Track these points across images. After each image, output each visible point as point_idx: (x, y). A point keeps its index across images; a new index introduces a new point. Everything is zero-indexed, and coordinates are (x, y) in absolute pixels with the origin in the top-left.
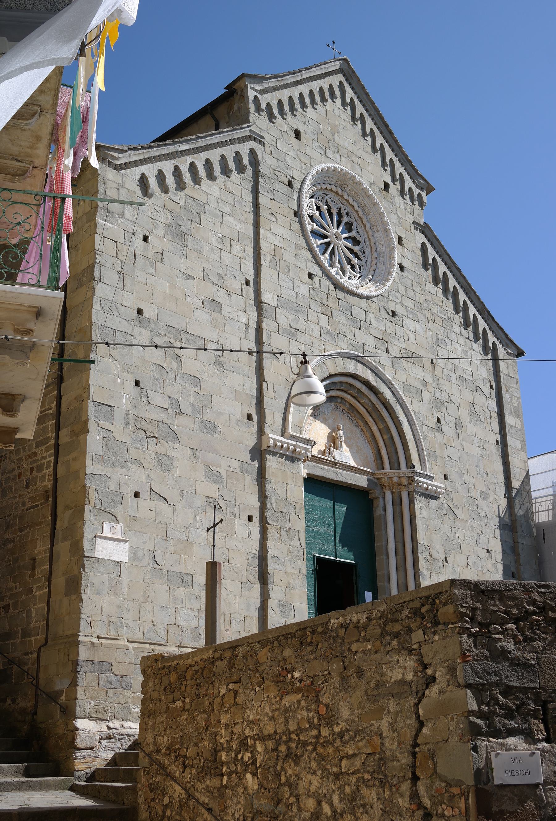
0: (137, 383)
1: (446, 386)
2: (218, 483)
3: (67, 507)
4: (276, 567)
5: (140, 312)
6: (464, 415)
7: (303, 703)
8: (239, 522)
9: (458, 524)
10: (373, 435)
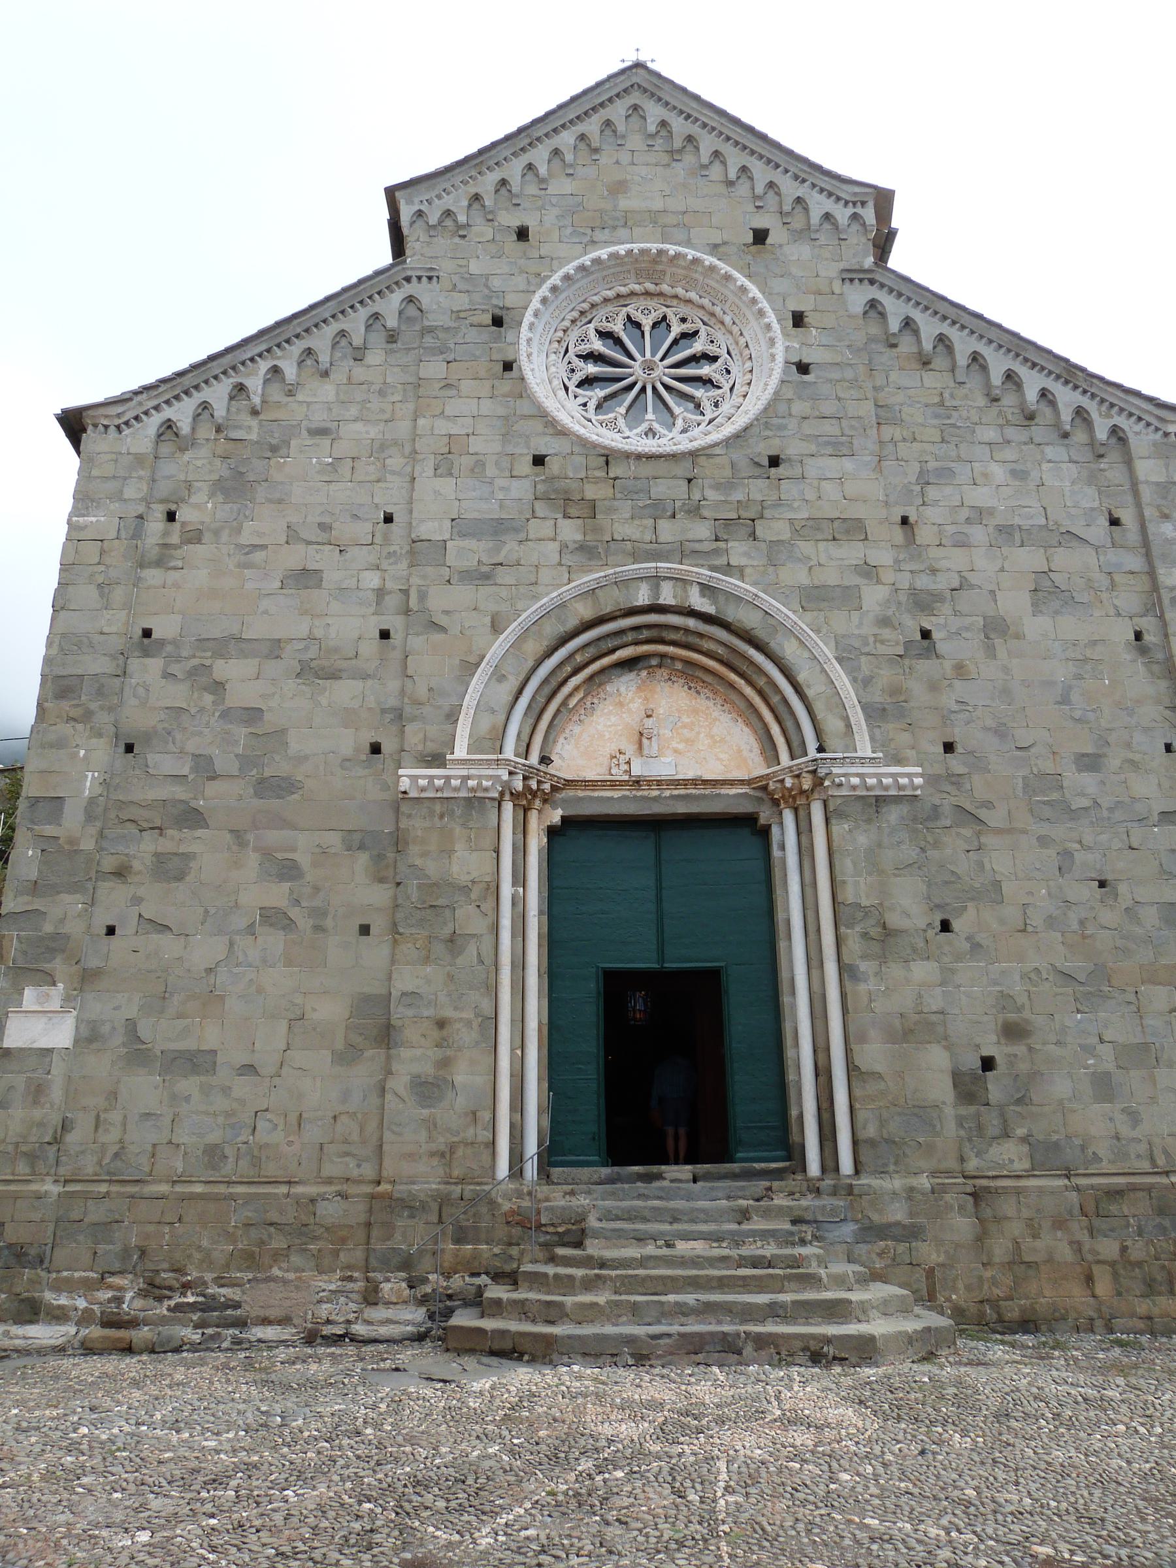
2: (292, 878)
5: (147, 633)
9: (988, 840)
10: (751, 705)
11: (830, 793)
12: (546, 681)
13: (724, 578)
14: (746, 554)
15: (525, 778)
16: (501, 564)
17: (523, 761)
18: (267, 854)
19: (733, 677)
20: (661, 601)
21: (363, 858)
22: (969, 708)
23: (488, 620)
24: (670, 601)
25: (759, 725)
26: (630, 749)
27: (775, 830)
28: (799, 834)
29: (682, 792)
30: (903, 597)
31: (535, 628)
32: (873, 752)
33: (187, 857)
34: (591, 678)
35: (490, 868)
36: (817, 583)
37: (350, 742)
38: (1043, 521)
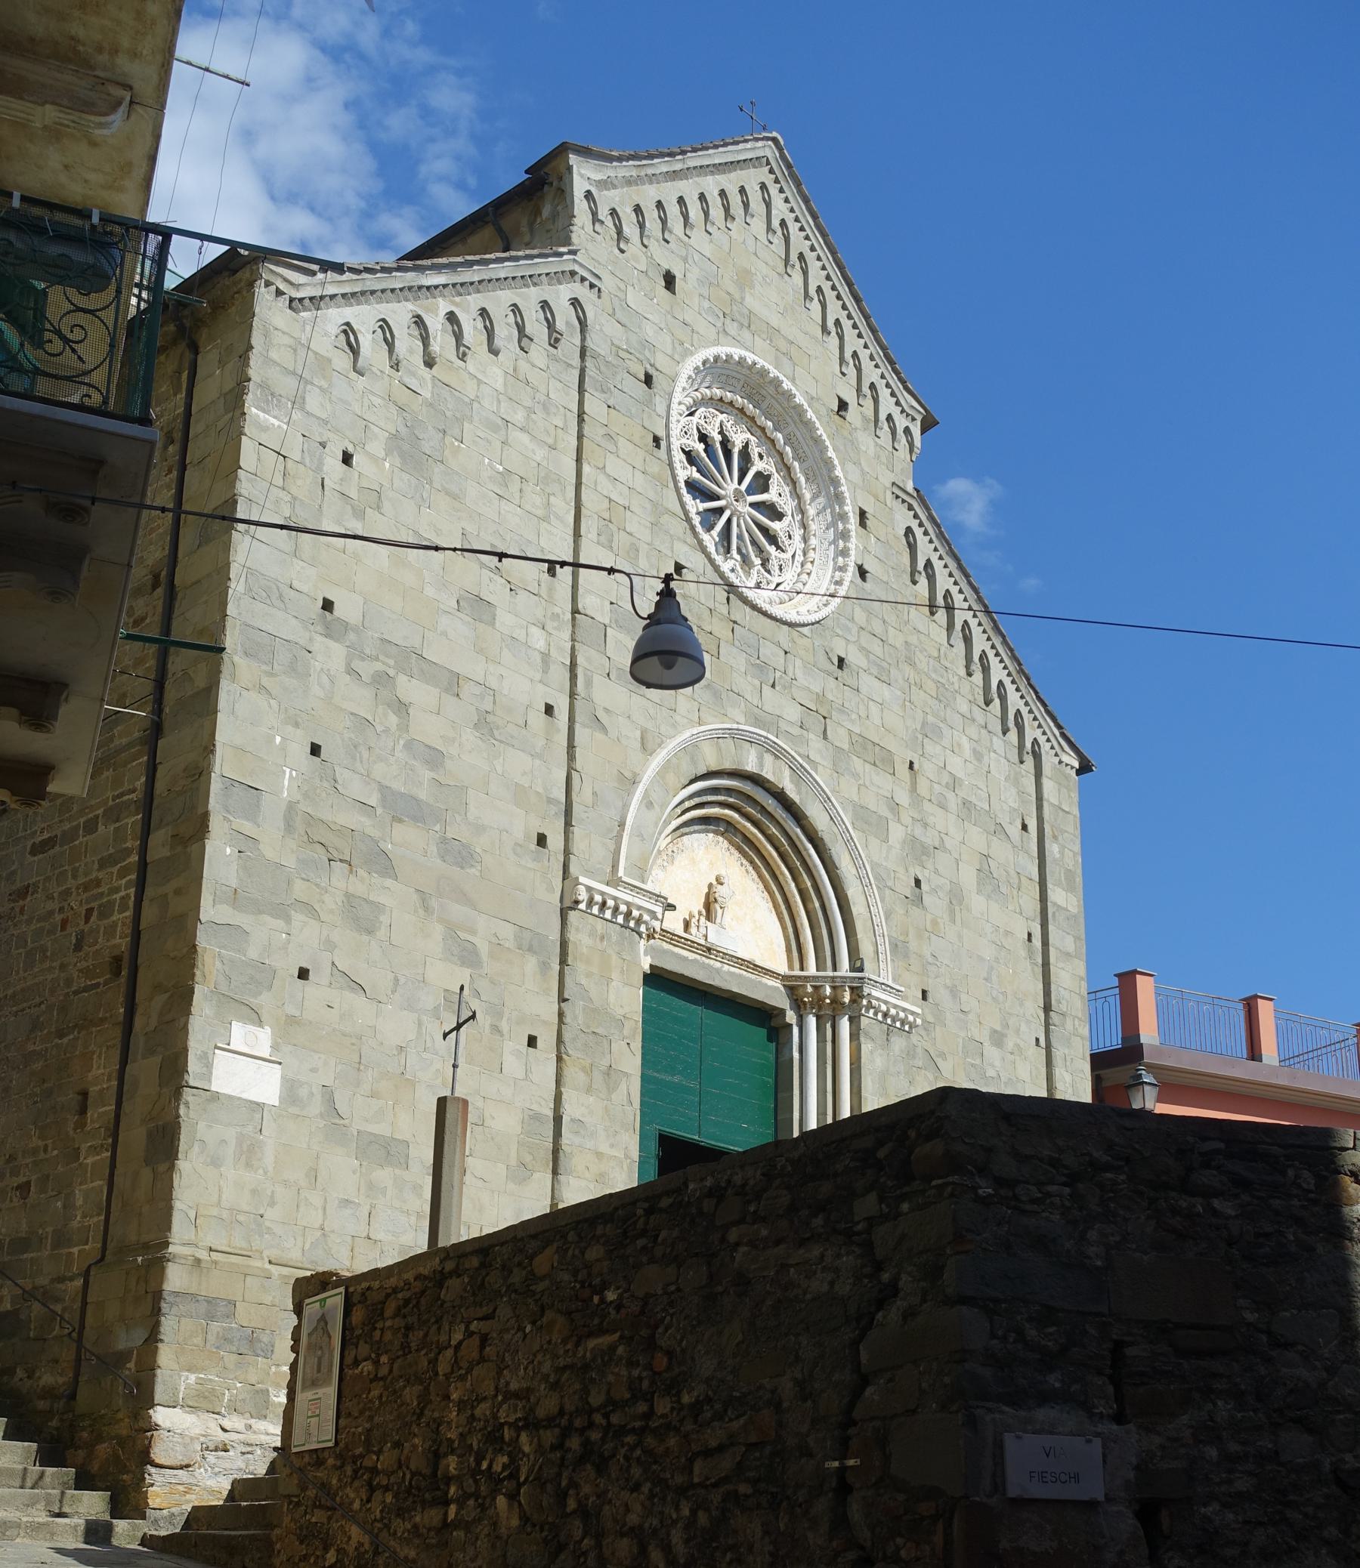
0: (315, 750)
1: (937, 818)
3: (158, 988)
4: (577, 1140)
6: (968, 876)
7: (620, 1350)
8: (509, 1046)
18: (452, 930)
21: (531, 963)
22: (938, 964)
33: (378, 907)
37: (522, 825)
38: (987, 808)
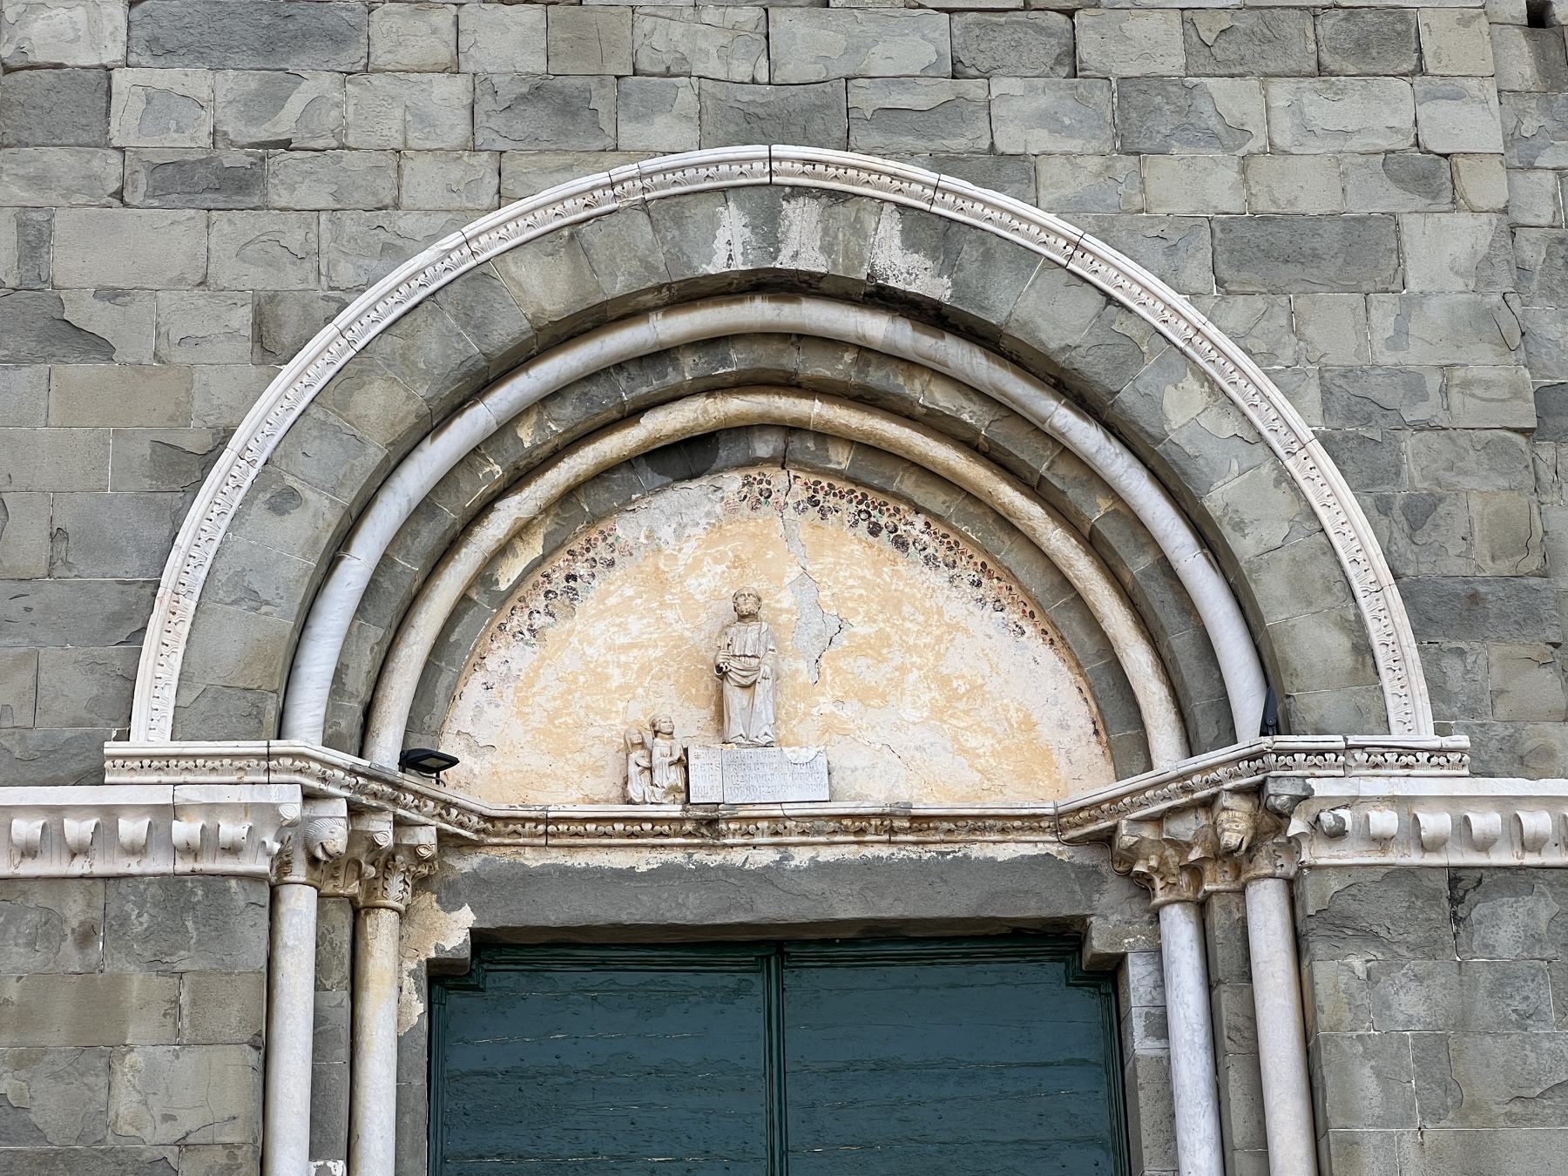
10: (1066, 584)
11: (1305, 857)
12: (424, 509)
13: (977, 191)
14: (1049, 120)
15: (355, 811)
16: (286, 145)
17: (350, 760)
19: (1008, 495)
20: (784, 262)
23: (242, 318)
24: (813, 261)
25: (1090, 645)
26: (690, 721)
27: (1137, 972)
28: (1211, 985)
29: (850, 853)
30: (1532, 251)
31: (393, 343)
32: (1440, 730)
34: (569, 495)
35: (236, 1097)
36: (1263, 205)
